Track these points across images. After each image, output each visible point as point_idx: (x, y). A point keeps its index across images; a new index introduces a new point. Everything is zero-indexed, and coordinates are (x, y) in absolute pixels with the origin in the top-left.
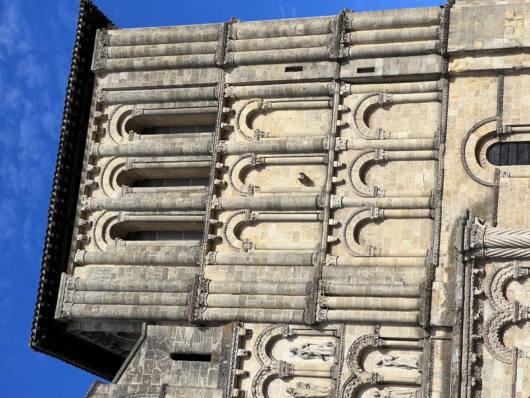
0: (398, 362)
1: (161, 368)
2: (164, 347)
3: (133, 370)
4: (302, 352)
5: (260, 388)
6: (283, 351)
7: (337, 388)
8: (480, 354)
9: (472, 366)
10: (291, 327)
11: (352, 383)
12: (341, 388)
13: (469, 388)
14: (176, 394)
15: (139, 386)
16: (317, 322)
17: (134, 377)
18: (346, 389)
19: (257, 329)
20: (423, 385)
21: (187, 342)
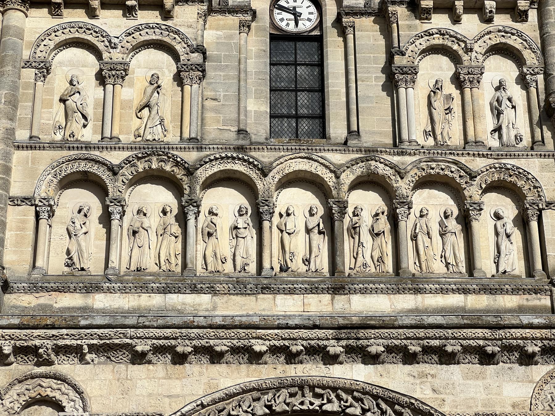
0: (504, 243)
4: (501, 98)
5: (437, 40)
6: (500, 69)
7: (452, 151)
8: (540, 360)
9: (518, 346)
10: (540, 78)
11: (463, 173)
12: (452, 157)
13: (481, 342)
18: (452, 166)
19: (530, 27)
20: (474, 281)
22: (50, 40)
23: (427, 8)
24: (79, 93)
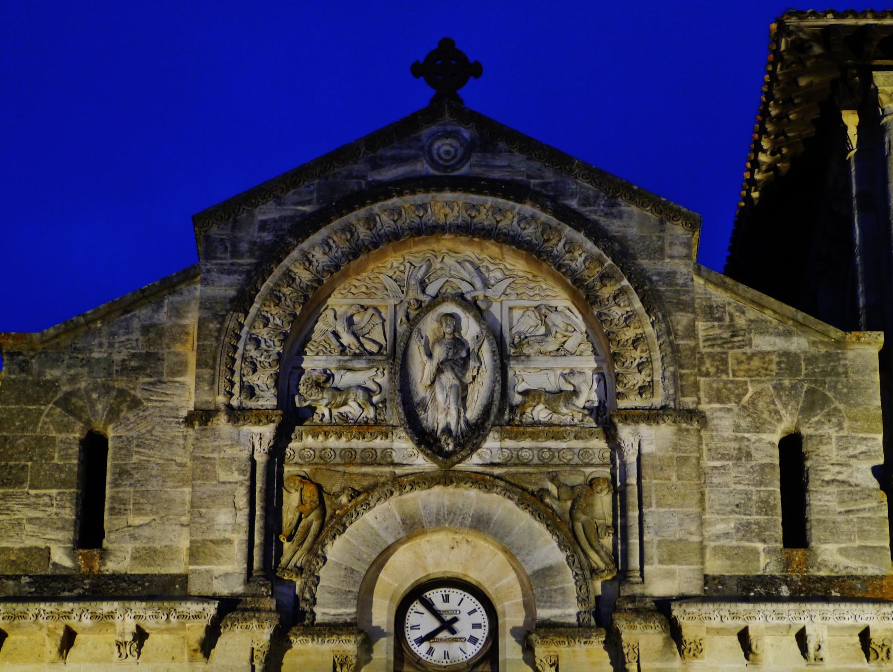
1: (753, 402)
3: (741, 322)
14: (676, 455)
15: (692, 343)
17: (720, 327)
21: (837, 469)
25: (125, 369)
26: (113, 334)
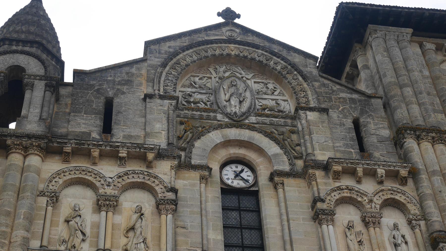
2: (363, 112)
3: (335, 89)
4: (396, 236)
5: (346, 194)
10: (422, 223)
14: (320, 120)
16: (438, 245)
21: (375, 131)
22: (59, 178)
23: (338, 171)
24: (80, 216)
25: (120, 83)
26: (115, 73)
